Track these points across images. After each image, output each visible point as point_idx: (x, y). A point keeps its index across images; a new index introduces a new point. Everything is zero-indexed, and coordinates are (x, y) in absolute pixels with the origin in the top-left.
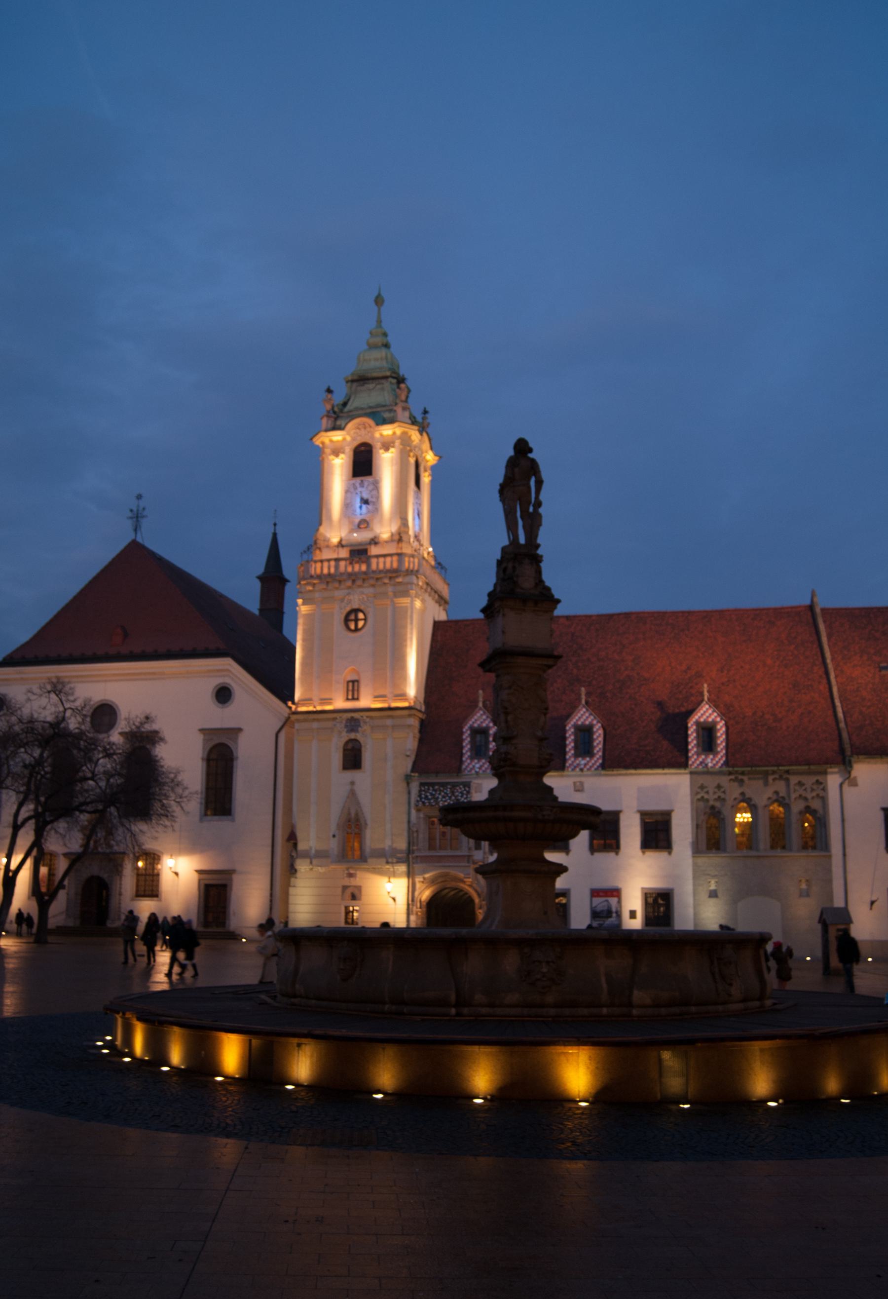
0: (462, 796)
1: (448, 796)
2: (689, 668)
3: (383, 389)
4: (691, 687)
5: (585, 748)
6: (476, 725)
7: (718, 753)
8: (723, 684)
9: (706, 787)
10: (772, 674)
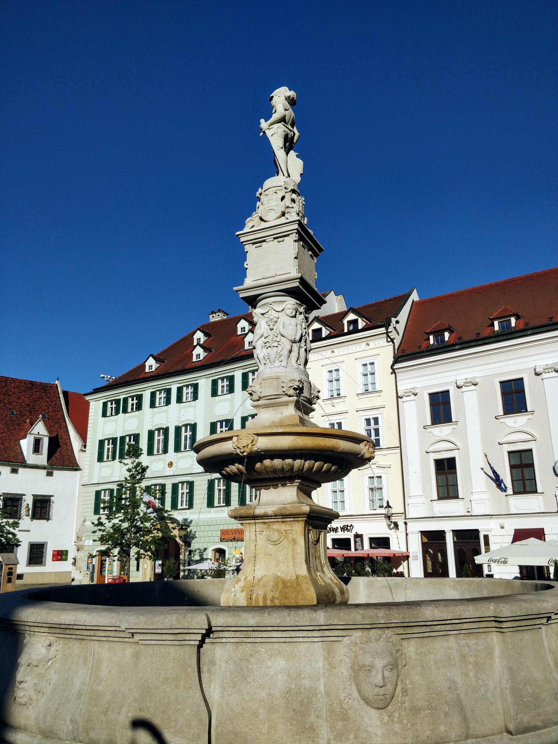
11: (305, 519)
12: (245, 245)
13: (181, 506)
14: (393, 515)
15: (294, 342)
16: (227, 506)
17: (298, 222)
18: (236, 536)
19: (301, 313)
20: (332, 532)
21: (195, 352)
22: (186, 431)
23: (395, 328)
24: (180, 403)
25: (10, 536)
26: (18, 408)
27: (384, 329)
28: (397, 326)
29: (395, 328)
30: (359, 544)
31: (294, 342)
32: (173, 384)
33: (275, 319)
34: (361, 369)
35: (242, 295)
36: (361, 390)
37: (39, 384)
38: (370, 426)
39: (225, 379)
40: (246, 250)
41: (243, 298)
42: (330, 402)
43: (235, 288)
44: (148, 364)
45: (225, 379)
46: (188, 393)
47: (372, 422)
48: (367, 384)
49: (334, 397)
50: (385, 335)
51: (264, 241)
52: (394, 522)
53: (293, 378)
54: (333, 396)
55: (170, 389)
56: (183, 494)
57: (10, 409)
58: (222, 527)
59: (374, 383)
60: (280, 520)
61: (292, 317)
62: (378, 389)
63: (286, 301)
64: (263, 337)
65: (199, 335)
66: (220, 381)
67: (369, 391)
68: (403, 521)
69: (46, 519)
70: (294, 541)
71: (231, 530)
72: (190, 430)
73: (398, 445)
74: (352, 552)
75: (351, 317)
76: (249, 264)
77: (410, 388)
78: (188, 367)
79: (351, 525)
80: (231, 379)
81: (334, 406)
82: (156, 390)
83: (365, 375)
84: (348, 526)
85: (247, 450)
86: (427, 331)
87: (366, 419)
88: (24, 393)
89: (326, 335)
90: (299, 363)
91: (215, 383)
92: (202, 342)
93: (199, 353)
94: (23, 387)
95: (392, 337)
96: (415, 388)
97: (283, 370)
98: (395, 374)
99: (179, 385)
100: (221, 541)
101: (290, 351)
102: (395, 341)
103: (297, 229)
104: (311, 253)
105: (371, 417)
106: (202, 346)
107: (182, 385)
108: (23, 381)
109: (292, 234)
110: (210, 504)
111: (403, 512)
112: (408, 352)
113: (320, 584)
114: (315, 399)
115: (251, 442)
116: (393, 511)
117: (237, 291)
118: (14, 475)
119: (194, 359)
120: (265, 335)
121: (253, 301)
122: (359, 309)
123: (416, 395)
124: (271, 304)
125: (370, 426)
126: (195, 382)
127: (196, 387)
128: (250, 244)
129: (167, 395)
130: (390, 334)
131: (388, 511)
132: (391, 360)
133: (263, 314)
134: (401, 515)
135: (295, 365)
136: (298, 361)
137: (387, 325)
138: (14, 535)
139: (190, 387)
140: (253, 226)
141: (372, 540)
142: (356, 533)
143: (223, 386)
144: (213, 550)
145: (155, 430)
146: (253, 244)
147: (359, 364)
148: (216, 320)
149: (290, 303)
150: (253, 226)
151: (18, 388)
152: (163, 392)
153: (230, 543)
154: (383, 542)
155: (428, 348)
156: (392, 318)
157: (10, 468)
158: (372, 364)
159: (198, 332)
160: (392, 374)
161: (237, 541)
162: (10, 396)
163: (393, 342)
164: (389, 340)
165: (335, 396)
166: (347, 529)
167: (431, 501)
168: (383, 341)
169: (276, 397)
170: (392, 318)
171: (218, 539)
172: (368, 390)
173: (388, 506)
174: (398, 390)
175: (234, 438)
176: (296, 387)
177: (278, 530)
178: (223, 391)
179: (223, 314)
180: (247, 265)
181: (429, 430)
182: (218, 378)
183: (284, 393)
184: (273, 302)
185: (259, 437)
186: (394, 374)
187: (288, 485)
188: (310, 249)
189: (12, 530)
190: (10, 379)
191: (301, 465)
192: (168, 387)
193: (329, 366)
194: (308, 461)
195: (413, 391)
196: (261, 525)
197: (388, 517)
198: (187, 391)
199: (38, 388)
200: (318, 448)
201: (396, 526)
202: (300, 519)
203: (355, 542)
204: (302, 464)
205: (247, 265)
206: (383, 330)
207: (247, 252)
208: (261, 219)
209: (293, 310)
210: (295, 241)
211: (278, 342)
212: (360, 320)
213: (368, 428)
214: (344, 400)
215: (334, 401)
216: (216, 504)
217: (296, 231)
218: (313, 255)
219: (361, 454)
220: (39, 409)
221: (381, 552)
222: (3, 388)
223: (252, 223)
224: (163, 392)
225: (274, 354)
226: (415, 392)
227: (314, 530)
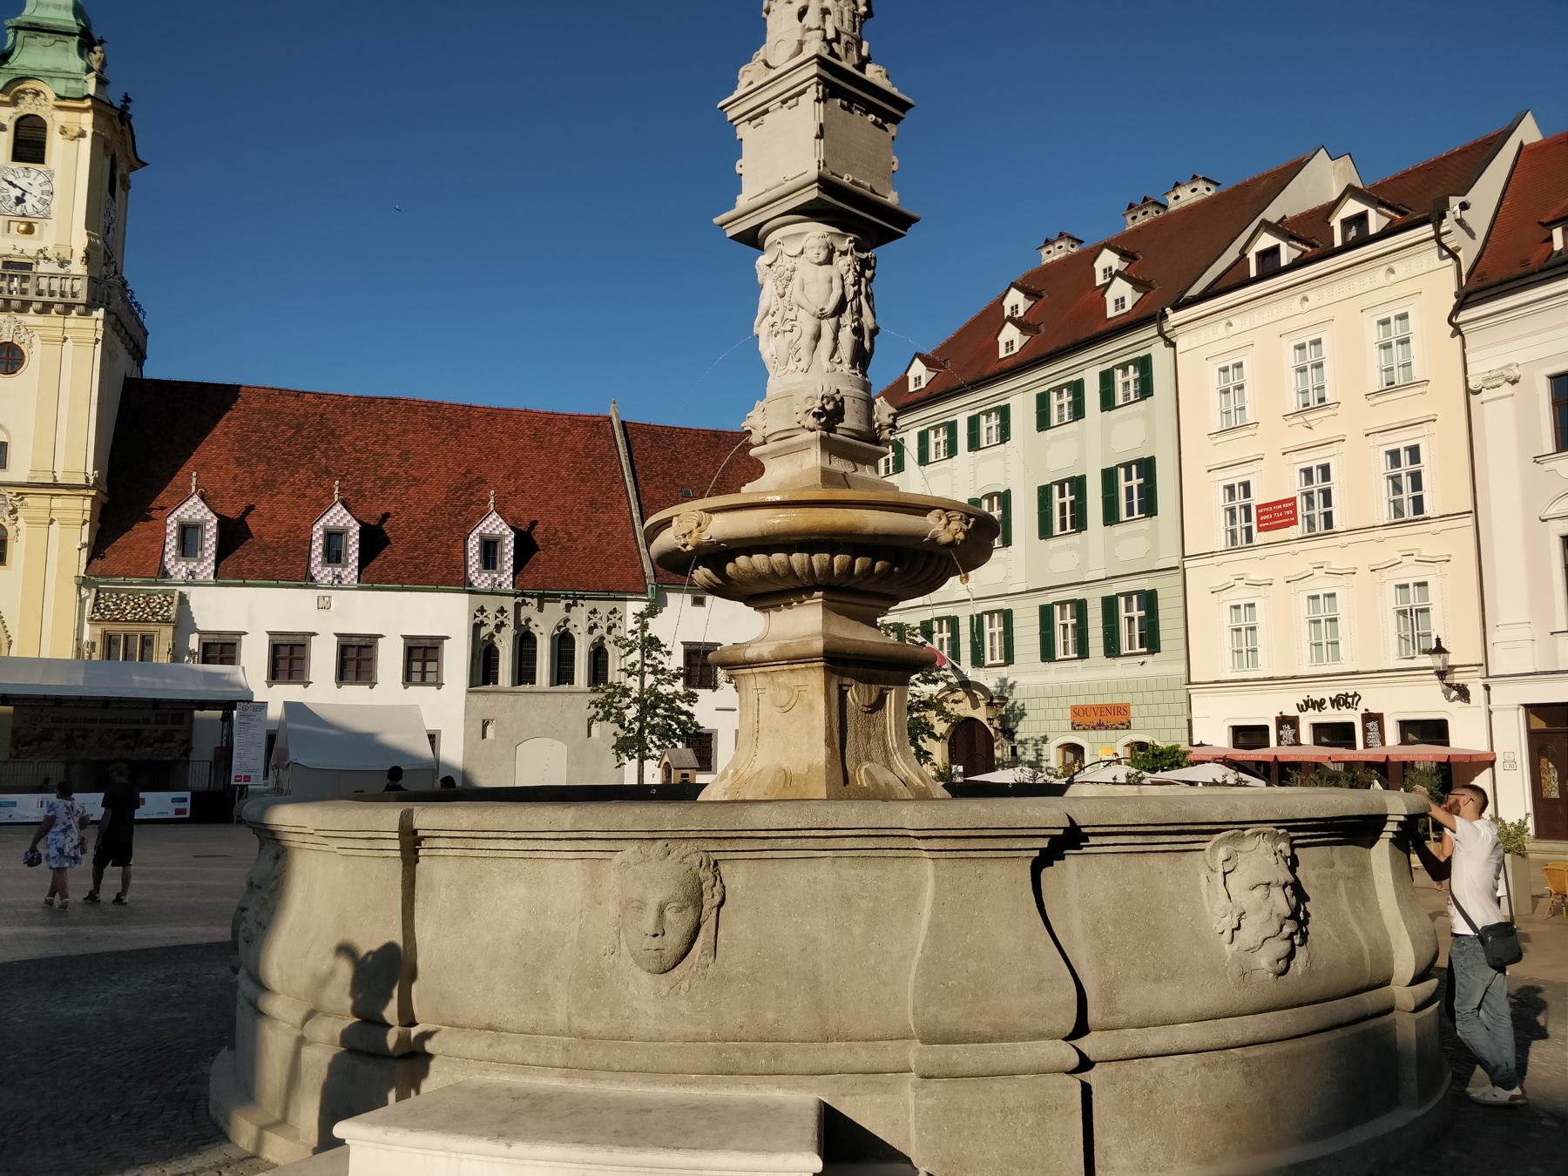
0: (161, 608)
1: (139, 605)
2: (469, 471)
3: (67, 50)
4: (472, 494)
5: (333, 554)
6: (186, 516)
7: (503, 572)
8: (509, 493)
9: (506, 612)
10: (566, 488)
11: (822, 664)
12: (736, 126)
13: (992, 659)
14: (1457, 670)
15: (822, 316)
16: (1082, 658)
17: (816, 60)
18: (1104, 720)
19: (844, 253)
20: (1310, 710)
23: (1460, 222)
24: (976, 450)
25: (683, 718)
26: (695, 485)
27: (1430, 226)
28: (1466, 215)
29: (1460, 222)
30: (1374, 733)
31: (822, 316)
32: (960, 411)
33: (787, 274)
34: (1375, 334)
35: (730, 233)
36: (1377, 383)
37: (729, 435)
38: (1400, 466)
40: (738, 137)
41: (735, 238)
42: (1300, 419)
43: (717, 220)
44: (912, 374)
45: (1065, 390)
46: (991, 428)
47: (1405, 457)
49: (1311, 406)
50: (1434, 243)
51: (766, 112)
52: (1458, 684)
53: (809, 394)
54: (1308, 404)
55: (955, 422)
56: (992, 635)
57: (683, 487)
58: (1073, 702)
60: (785, 667)
61: (820, 264)
62: (1417, 375)
63: (807, 233)
64: (769, 316)
65: (1016, 300)
66: (1054, 395)
67: (1396, 384)
68: (1481, 682)
69: (710, 687)
70: (811, 707)
71: (1093, 708)
72: (998, 504)
73: (1470, 507)
74: (1360, 751)
75: (1352, 207)
76: (744, 166)
77: (1499, 367)
79: (1356, 694)
80: (1077, 388)
81: (1310, 428)
83: (1387, 346)
84: (1347, 695)
85: (692, 541)
86: (1545, 220)
88: (704, 455)
90: (839, 360)
91: (1043, 401)
93: (1011, 337)
94: (700, 443)
95: (1450, 246)
96: (1510, 365)
97: (800, 377)
98: (1462, 335)
99: (972, 413)
100: (1074, 729)
101: (817, 337)
102: (1460, 254)
103: (817, 75)
104: (874, 117)
105: (1401, 446)
106: (1018, 323)
108: (701, 432)
109: (809, 86)
110: (1047, 654)
111: (1480, 660)
112: (1495, 279)
113: (859, 783)
114: (887, 431)
115: (696, 525)
116: (1452, 661)
117: (722, 225)
118: (698, 609)
119: (1002, 354)
120: (771, 311)
121: (753, 239)
123: (1514, 382)
124: (780, 243)
125: (1400, 466)
126: (1002, 403)
127: (1004, 412)
128: (744, 122)
129: (949, 436)
130: (1444, 240)
131: (1445, 661)
133: (770, 266)
134: (1475, 668)
135: (826, 364)
136: (836, 356)
137: (1437, 217)
138: (690, 716)
139: (993, 414)
140: (751, 83)
141: (1406, 726)
142: (1366, 710)
144: (1059, 747)
146: (750, 120)
148: (1055, 258)
149: (816, 233)
150: (751, 83)
151: (693, 446)
153: (1093, 733)
154: (1435, 731)
155: (1547, 260)
157: (690, 595)
160: (1453, 335)
161: (1106, 728)
162: (680, 462)
163: (1456, 258)
164: (1445, 253)
165: (1314, 403)
166: (1345, 703)
167: (1552, 633)
168: (1430, 257)
169: (787, 434)
171: (1067, 725)
172: (1393, 383)
173: (1439, 650)
176: (816, 410)
177: (786, 687)
178: (1061, 417)
179: (1070, 243)
180: (741, 166)
181: (1548, 466)
182: (1050, 390)
183: (800, 426)
184: (783, 238)
185: (712, 516)
186: (1458, 337)
187: (806, 602)
188: (869, 108)
189: (685, 707)
190: (678, 430)
191: (803, 564)
192: (949, 420)
193: (1296, 335)
194: (816, 556)
195: (1508, 374)
196: (760, 678)
197: (1441, 674)
198: (989, 425)
199: (728, 442)
200: (818, 530)
201: (1464, 693)
202: (816, 664)
203: (1366, 731)
204: (806, 561)
205: (741, 166)
206: (1427, 230)
207: (741, 140)
208: (767, 65)
209: (821, 249)
210: (818, 100)
211: (792, 320)
213: (1396, 471)
214: (1335, 412)
215: (1308, 417)
216: (1059, 654)
217: (815, 79)
218: (880, 120)
219: (929, 536)
220: (733, 483)
221: (1425, 754)
222: (667, 448)
223: (751, 75)
225: (785, 347)
227: (861, 685)
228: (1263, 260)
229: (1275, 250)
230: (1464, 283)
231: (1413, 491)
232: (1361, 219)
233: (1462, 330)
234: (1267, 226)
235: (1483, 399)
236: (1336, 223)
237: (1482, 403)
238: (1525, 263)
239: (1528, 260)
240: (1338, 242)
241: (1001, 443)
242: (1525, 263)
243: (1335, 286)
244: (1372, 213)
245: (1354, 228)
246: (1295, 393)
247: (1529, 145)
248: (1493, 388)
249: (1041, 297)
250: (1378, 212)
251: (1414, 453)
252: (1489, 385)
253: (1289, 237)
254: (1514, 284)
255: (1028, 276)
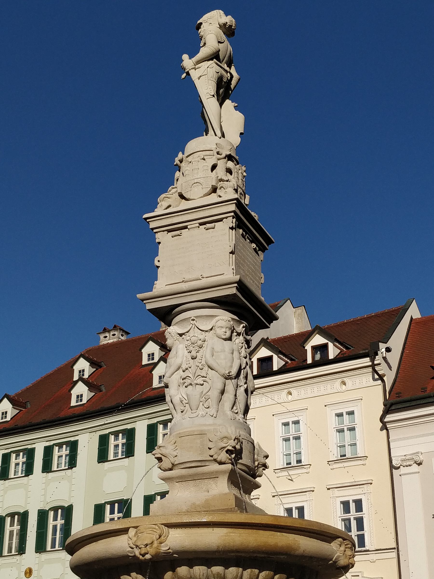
21: (75, 392)
22: (55, 519)
23: (385, 358)
24: (48, 472)
27: (368, 359)
28: (389, 356)
29: (385, 358)
34: (333, 422)
36: (335, 454)
38: (350, 513)
39: (121, 435)
42: (285, 473)
45: (121, 435)
46: (62, 456)
47: (352, 506)
48: (344, 446)
49: (292, 465)
50: (370, 369)
54: (290, 464)
59: (355, 444)
62: (360, 453)
66: (112, 437)
67: (347, 456)
72: (61, 516)
78: (62, 414)
81: (292, 480)
82: (11, 452)
83: (341, 431)
87: (342, 503)
89: (280, 367)
92: (86, 376)
95: (380, 373)
98: (387, 430)
102: (385, 378)
105: (350, 499)
106: (86, 382)
107: (52, 443)
112: (406, 397)
122: (329, 328)
125: (350, 513)
130: (377, 368)
132: (380, 408)
139: (64, 446)
143: (116, 446)
145: (6, 516)
147: (331, 413)
152: (21, 454)
156: (380, 343)
158: (351, 413)
159: (82, 360)
160: (382, 429)
163: (383, 381)
164: (376, 377)
165: (294, 463)
170: (380, 343)
172: (345, 456)
174: (392, 456)
175: (130, 530)
178: (116, 454)
182: (110, 433)
186: (385, 430)
198: (60, 454)
206: (366, 361)
212: (331, 346)
213: (347, 516)
215: (291, 472)
224: (21, 454)
226: (418, 459)
228: (262, 364)
229: (270, 359)
230: (387, 398)
231: (358, 531)
232: (323, 348)
233: (388, 426)
234: (265, 342)
235: (400, 473)
236: (308, 348)
237: (400, 475)
238: (424, 390)
239: (426, 388)
240: (309, 361)
241: (68, 469)
242: (424, 390)
243: (315, 387)
244: (331, 346)
245: (319, 352)
246: (282, 455)
247: (416, 319)
248: (407, 466)
249: (101, 367)
250: (334, 345)
251: (359, 504)
252: (405, 464)
253: (279, 352)
254: (419, 402)
255: (90, 350)
